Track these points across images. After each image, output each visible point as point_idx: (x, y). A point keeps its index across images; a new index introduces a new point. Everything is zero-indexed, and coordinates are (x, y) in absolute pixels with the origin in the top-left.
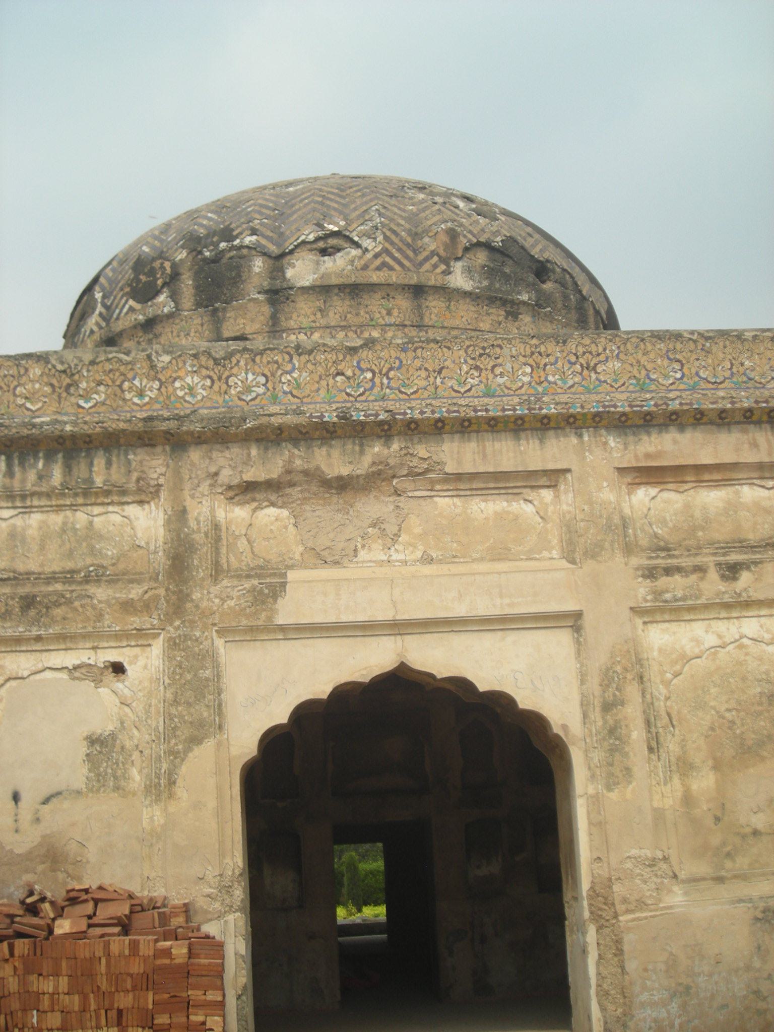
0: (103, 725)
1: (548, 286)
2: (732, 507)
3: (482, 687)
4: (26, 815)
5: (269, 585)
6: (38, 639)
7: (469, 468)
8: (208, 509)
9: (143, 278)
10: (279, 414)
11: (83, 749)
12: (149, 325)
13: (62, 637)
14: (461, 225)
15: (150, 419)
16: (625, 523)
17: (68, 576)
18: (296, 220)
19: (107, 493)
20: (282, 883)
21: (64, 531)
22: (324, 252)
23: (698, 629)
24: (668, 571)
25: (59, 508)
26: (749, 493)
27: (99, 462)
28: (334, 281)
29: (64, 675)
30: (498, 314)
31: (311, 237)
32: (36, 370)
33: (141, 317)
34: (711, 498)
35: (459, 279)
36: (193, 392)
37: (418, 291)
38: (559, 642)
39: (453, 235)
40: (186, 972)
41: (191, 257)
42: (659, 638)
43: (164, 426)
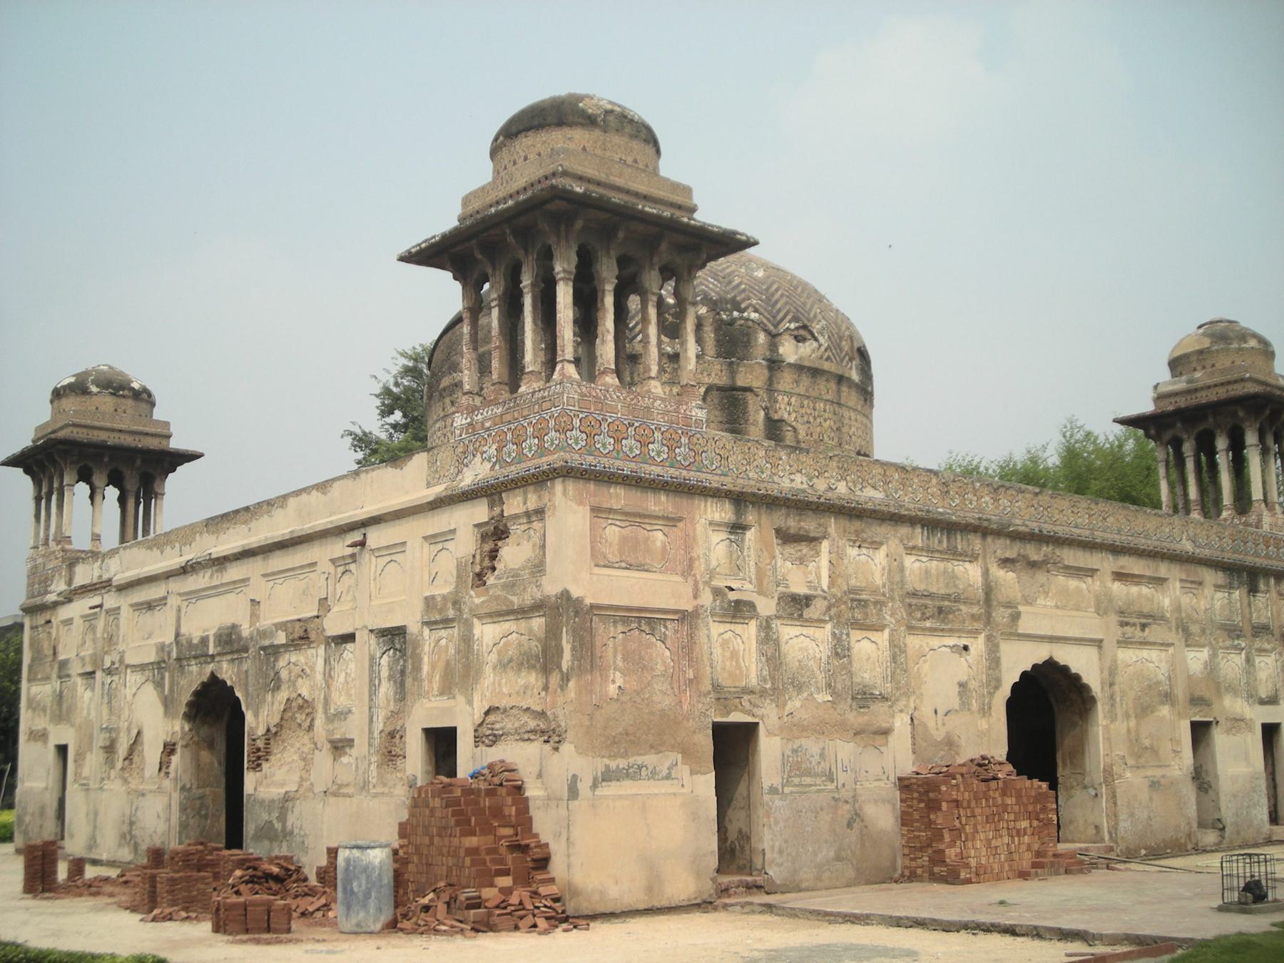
0: (964, 678)
2: (1140, 595)
3: (1073, 671)
4: (940, 722)
6: (942, 630)
7: (1071, 564)
11: (957, 689)
13: (951, 630)
15: (979, 519)
17: (946, 597)
18: (779, 311)
19: (961, 555)
21: (945, 572)
24: (1127, 624)
25: (943, 560)
26: (1145, 590)
28: (807, 364)
29: (948, 650)
31: (792, 326)
32: (934, 481)
33: (669, 349)
34: (1134, 590)
35: (855, 376)
37: (840, 379)
41: (711, 314)
43: (985, 524)
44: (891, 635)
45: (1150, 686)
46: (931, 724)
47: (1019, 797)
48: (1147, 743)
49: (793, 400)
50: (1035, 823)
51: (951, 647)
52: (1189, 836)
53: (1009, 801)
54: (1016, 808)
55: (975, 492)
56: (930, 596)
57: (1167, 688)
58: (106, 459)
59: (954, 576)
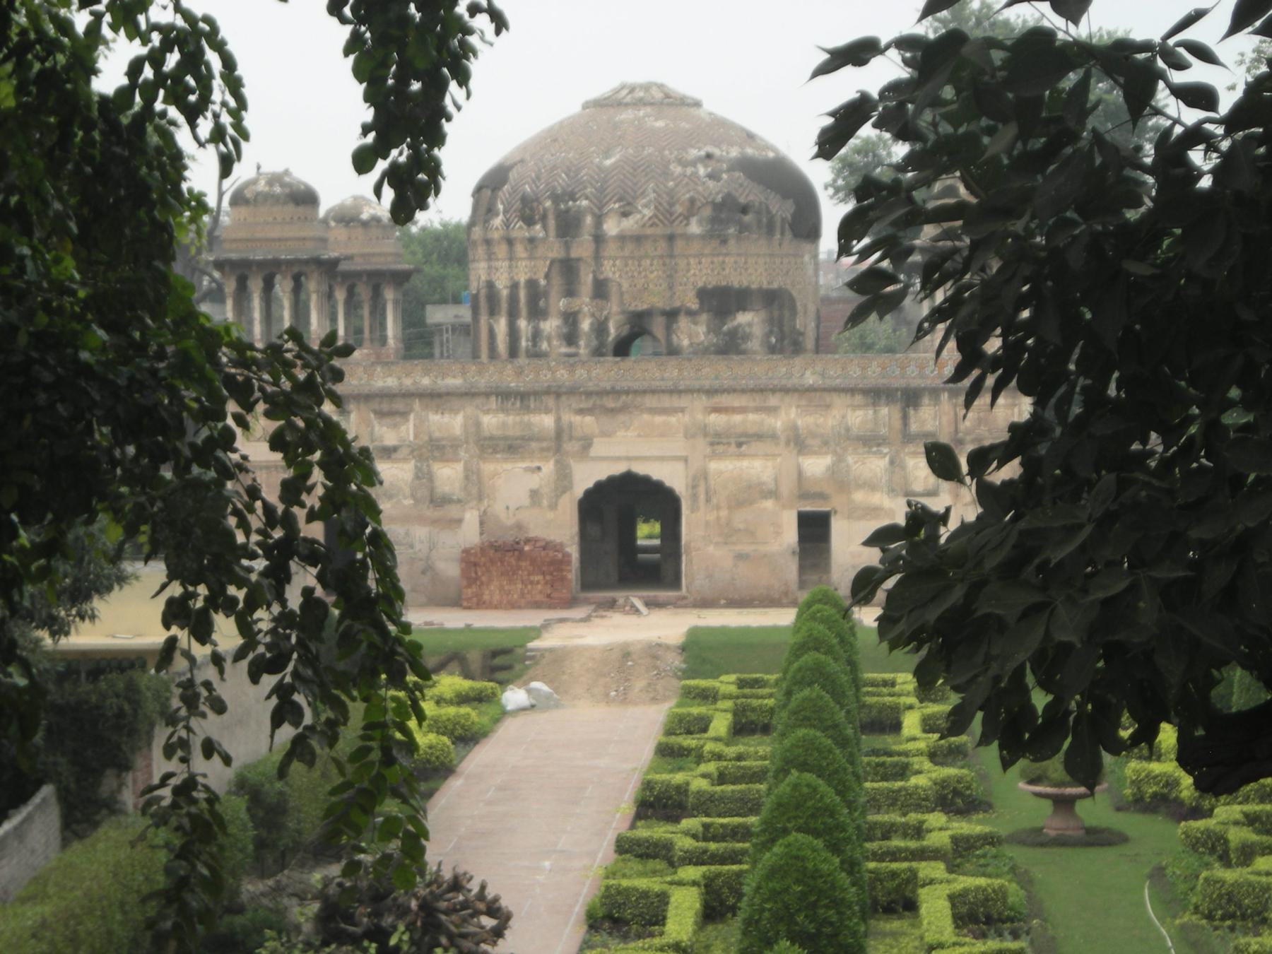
0: (534, 485)
1: (748, 218)
5: (587, 443)
8: (569, 417)
9: (528, 211)
10: (591, 386)
12: (532, 240)
14: (698, 192)
16: (705, 426)
17: (522, 438)
20: (595, 530)
22: (625, 215)
23: (727, 463)
27: (532, 398)
30: (715, 243)
31: (617, 206)
32: (509, 366)
34: (737, 418)
36: (563, 375)
37: (671, 238)
38: (680, 466)
39: (692, 201)
40: (561, 562)
42: (714, 466)
44: (466, 464)
45: (750, 487)
46: (503, 516)
47: (533, 561)
48: (741, 526)
49: (618, 262)
50: (548, 578)
51: (527, 469)
52: (786, 594)
53: (523, 564)
54: (531, 568)
55: (549, 369)
56: (505, 438)
57: (772, 486)
58: (339, 279)
59: (529, 425)
